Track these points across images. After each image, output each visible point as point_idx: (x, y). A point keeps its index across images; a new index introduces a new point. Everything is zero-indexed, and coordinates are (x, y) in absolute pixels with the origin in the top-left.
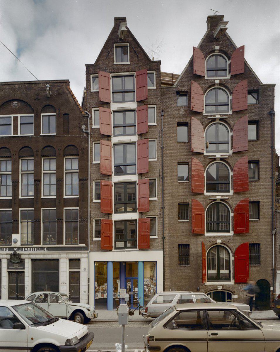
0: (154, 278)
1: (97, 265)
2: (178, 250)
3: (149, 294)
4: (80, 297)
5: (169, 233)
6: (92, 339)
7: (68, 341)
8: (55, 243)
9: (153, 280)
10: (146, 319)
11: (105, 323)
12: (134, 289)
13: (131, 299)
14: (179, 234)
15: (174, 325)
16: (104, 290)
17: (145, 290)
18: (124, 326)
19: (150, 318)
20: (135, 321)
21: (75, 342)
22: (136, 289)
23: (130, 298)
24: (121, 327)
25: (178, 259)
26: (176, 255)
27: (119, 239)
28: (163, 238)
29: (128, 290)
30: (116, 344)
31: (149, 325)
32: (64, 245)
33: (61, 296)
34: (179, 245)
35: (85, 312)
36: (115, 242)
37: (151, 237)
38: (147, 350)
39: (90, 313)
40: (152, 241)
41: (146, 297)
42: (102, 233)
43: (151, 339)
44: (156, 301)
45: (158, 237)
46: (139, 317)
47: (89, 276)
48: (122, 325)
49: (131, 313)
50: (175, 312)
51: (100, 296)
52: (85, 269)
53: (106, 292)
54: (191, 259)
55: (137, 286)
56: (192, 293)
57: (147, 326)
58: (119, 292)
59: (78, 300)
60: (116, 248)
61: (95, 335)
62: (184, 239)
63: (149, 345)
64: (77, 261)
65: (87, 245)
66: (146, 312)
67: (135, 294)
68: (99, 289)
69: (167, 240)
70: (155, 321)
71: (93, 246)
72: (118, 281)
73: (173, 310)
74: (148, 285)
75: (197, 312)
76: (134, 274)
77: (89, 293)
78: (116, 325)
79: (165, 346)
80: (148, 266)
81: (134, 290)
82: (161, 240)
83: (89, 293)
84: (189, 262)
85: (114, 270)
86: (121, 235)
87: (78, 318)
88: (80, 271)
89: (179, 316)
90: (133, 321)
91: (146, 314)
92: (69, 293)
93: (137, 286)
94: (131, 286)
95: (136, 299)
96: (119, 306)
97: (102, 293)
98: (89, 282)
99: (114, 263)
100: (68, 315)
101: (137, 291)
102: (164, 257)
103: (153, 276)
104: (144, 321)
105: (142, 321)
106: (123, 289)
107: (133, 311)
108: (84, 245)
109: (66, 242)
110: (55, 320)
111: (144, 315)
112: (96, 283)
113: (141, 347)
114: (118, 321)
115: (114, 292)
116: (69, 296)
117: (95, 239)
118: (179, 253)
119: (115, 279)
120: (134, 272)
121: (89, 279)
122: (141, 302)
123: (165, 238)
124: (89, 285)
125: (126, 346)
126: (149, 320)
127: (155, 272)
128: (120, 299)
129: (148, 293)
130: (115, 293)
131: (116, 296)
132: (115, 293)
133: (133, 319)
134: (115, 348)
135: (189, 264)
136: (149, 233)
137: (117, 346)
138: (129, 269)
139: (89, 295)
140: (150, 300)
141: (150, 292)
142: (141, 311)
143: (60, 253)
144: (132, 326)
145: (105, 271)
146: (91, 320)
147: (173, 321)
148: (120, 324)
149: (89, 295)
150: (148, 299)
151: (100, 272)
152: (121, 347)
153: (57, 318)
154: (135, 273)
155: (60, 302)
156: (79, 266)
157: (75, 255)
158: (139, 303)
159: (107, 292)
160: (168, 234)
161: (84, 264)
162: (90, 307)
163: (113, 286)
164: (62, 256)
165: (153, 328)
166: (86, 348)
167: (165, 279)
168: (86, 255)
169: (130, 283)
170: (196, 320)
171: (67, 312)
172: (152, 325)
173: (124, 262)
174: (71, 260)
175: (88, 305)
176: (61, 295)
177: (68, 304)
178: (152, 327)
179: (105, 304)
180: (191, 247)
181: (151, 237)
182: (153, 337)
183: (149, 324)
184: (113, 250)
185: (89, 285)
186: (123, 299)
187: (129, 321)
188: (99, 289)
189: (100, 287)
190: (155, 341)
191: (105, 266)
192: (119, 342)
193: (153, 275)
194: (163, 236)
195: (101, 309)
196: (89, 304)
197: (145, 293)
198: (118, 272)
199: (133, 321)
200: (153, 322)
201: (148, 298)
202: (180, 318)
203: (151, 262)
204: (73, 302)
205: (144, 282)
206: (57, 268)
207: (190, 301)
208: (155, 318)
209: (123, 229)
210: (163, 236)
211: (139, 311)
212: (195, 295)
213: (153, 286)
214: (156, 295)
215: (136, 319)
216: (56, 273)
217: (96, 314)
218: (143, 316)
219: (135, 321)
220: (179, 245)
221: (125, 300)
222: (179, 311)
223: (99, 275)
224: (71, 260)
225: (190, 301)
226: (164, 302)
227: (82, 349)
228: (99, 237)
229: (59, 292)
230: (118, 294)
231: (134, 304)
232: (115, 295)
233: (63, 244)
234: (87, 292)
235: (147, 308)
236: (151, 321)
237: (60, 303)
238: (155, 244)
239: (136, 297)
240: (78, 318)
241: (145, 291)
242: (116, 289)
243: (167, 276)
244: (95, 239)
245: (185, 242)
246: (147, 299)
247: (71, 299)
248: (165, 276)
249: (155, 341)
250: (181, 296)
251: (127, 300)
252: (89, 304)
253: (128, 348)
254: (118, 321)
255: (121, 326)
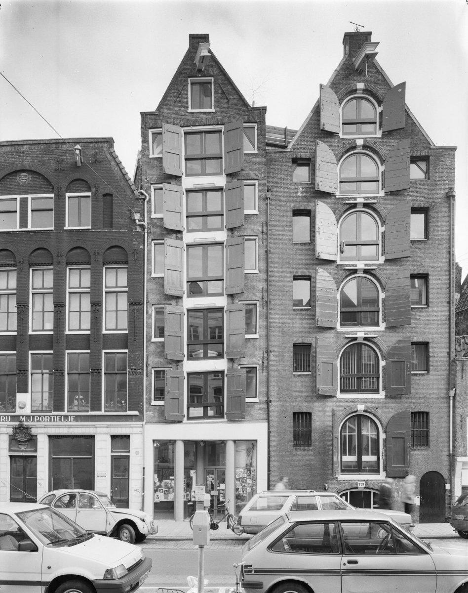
0: (252, 469)
1: (157, 445)
2: (292, 421)
3: (244, 495)
4: (128, 498)
5: (278, 394)
6: (149, 568)
7: (109, 572)
8: (87, 409)
9: (250, 471)
10: (239, 536)
11: (171, 541)
12: (219, 486)
13: (214, 502)
14: (294, 396)
15: (286, 547)
16: (169, 488)
17: (238, 487)
18: (201, 547)
19: (245, 535)
20: (220, 540)
21: (120, 574)
22: (222, 486)
23: (212, 501)
24: (197, 549)
25: (292, 436)
26: (290, 430)
27: (194, 402)
28: (268, 402)
29: (209, 488)
30: (189, 578)
31: (244, 546)
32: (102, 413)
33: (97, 496)
34: (295, 414)
35: (136, 524)
36: (188, 408)
37: (248, 400)
38: (241, 589)
39: (145, 526)
40: (249, 407)
41: (239, 499)
42: (166, 393)
43: (246, 569)
44: (255, 506)
45: (260, 400)
46: (227, 533)
47: (144, 464)
48: (200, 545)
49: (214, 527)
50: (287, 526)
51: (162, 498)
52: (137, 453)
53: (171, 490)
54: (314, 436)
55: (223, 481)
56: (315, 493)
57: (240, 547)
58: (194, 492)
59: (125, 504)
60: (189, 418)
61: (153, 562)
62: (302, 403)
63: (243, 580)
64: (125, 439)
65: (141, 413)
66: (239, 524)
67: (222, 495)
68: (160, 486)
69: (273, 406)
70: (253, 539)
71: (151, 414)
72: (192, 473)
73: (284, 521)
74: (243, 480)
75: (323, 525)
76: (219, 461)
77: (143, 492)
78: (188, 545)
79: (269, 581)
80: (243, 447)
81: (218, 488)
82: (264, 405)
83: (143, 492)
84: (310, 441)
85: (187, 454)
86: (198, 397)
87: (125, 534)
88: (129, 456)
89: (294, 531)
90: (216, 540)
91: (238, 528)
92: (111, 493)
93: (223, 481)
94: (213, 481)
95: (223, 502)
96: (194, 514)
97: (166, 493)
98: (144, 475)
99: (187, 443)
100: (110, 529)
101: (223, 490)
102: (269, 432)
103: (251, 465)
104: (236, 540)
105: (232, 539)
106: (200, 487)
107: (217, 523)
108: (136, 413)
109: (106, 407)
110: (87, 537)
111: (235, 530)
112: (156, 476)
113: (230, 583)
114: (192, 540)
115: (185, 491)
116: (111, 497)
117: (154, 403)
118: (295, 426)
119: (187, 470)
120: (218, 458)
121: (144, 468)
122: (231, 507)
123: (270, 402)
124: (144, 478)
125: (206, 582)
126: (244, 538)
127: (255, 457)
128: (195, 502)
129: (242, 492)
130: (188, 493)
131: (189, 498)
132: (188, 493)
133: (217, 537)
134: (187, 585)
135: (310, 445)
136: (244, 392)
137: (190, 580)
138: (210, 453)
139: (143, 496)
140: (245, 505)
141: (245, 492)
142: (230, 523)
143: (96, 426)
144: (215, 548)
145: (170, 457)
146: (147, 537)
147: (284, 540)
148: (195, 544)
149: (143, 496)
150: (242, 503)
151: (163, 458)
152: (196, 583)
153: (90, 534)
154: (221, 459)
155: (95, 507)
156: (127, 448)
157: (121, 429)
158: (227, 510)
159: (174, 491)
160: (276, 396)
161: (135, 443)
162: (146, 516)
163: (184, 481)
164: (99, 430)
165: (252, 551)
166: (138, 583)
167: (271, 469)
168: (140, 429)
169: (213, 476)
170: (322, 537)
171: (107, 524)
172: (249, 546)
173: (202, 441)
174: (114, 437)
175: (142, 512)
176: (98, 495)
177: (109, 510)
178: (249, 549)
179: (171, 510)
180: (314, 417)
181: (248, 400)
182: (251, 566)
183: (243, 544)
184: (183, 422)
185: (144, 478)
186: (201, 502)
187: (210, 540)
188: (160, 486)
189: (163, 483)
190: (253, 573)
191: (170, 447)
192: (194, 575)
193: (251, 463)
194: (268, 398)
195: (163, 519)
196: (143, 511)
197: (237, 493)
198: (192, 458)
199: (216, 540)
200: (251, 542)
201: (243, 500)
202: (295, 535)
203: (248, 442)
204: (117, 507)
205: (235, 474)
206: (91, 450)
207: (312, 507)
208: (253, 535)
209: (202, 387)
210: (268, 398)
211: (226, 522)
212: (321, 496)
213: (251, 482)
214: (256, 497)
215: (222, 537)
216: (90, 458)
217: (155, 527)
218: (233, 531)
219: (220, 540)
220: (295, 414)
221: (203, 505)
222: (293, 523)
223: (160, 462)
224: (114, 437)
225: (312, 507)
226: (269, 508)
227: (131, 585)
228: (162, 399)
229: (94, 490)
230: (193, 494)
231: (219, 511)
232: (187, 496)
233: (100, 410)
234: (141, 490)
235: (240, 518)
236: (247, 540)
237: (94, 508)
238: (254, 411)
239: (221, 499)
240: (125, 533)
241: (237, 490)
242: (188, 486)
243: (274, 464)
244: (154, 403)
245: (304, 409)
246: (240, 503)
247: (113, 501)
248: (271, 465)
249: (253, 573)
250: (297, 497)
251: (207, 504)
252: (143, 511)
253: (209, 585)
254: (192, 540)
255: (197, 547)
